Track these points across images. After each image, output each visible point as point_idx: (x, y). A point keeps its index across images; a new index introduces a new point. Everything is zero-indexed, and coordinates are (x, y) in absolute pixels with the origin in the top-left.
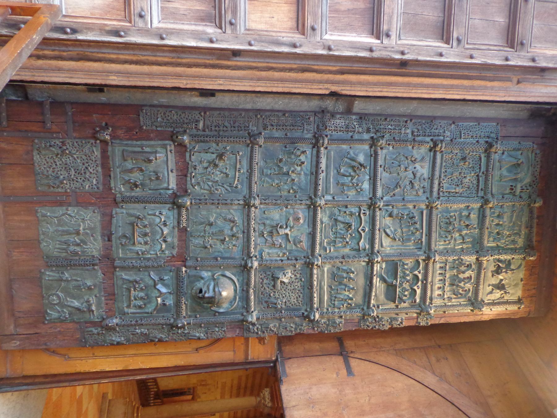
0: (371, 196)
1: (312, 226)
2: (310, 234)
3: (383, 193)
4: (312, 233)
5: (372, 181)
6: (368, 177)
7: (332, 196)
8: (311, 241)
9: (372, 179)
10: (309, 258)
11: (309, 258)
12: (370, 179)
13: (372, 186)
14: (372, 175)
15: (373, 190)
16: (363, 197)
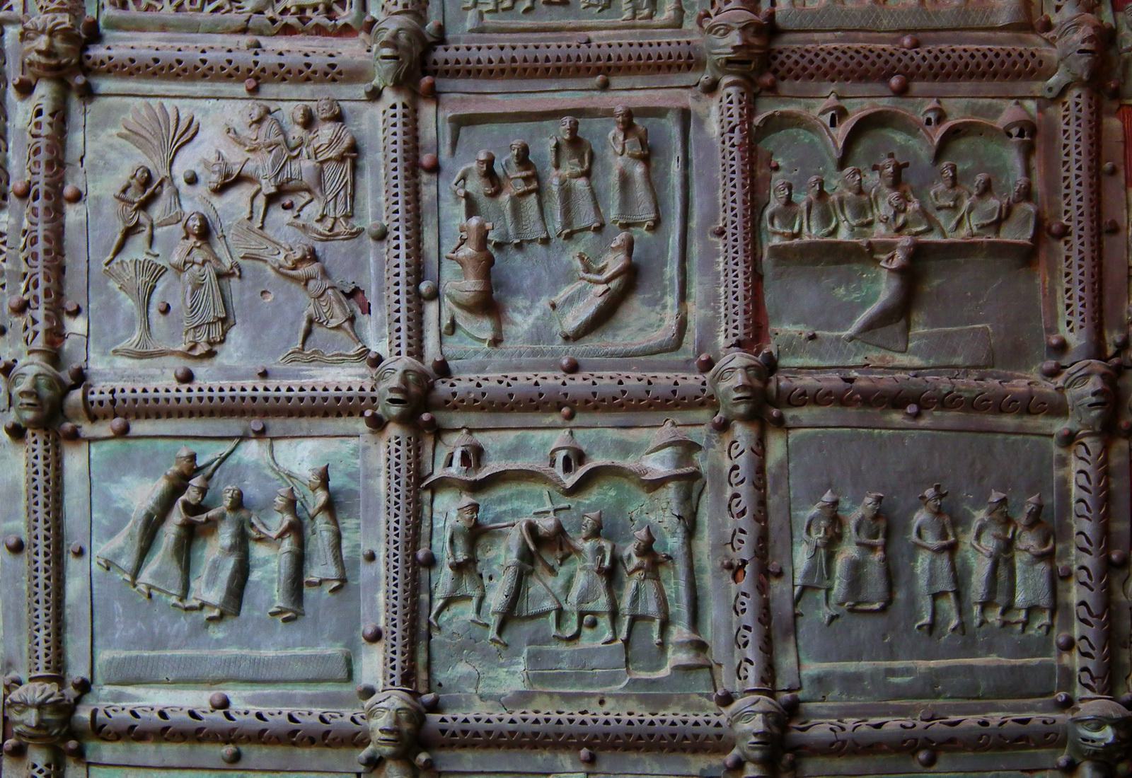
0: (361, 425)
1: (547, 754)
2: (592, 760)
3: (340, 360)
4: (584, 752)
5: (276, 425)
6: (252, 451)
7: (365, 647)
8: (633, 756)
9: (256, 424)
10: (739, 765)
11: (739, 765)
12: (261, 434)
13: (304, 423)
14: (234, 426)
15: (326, 414)
16: (370, 475)
